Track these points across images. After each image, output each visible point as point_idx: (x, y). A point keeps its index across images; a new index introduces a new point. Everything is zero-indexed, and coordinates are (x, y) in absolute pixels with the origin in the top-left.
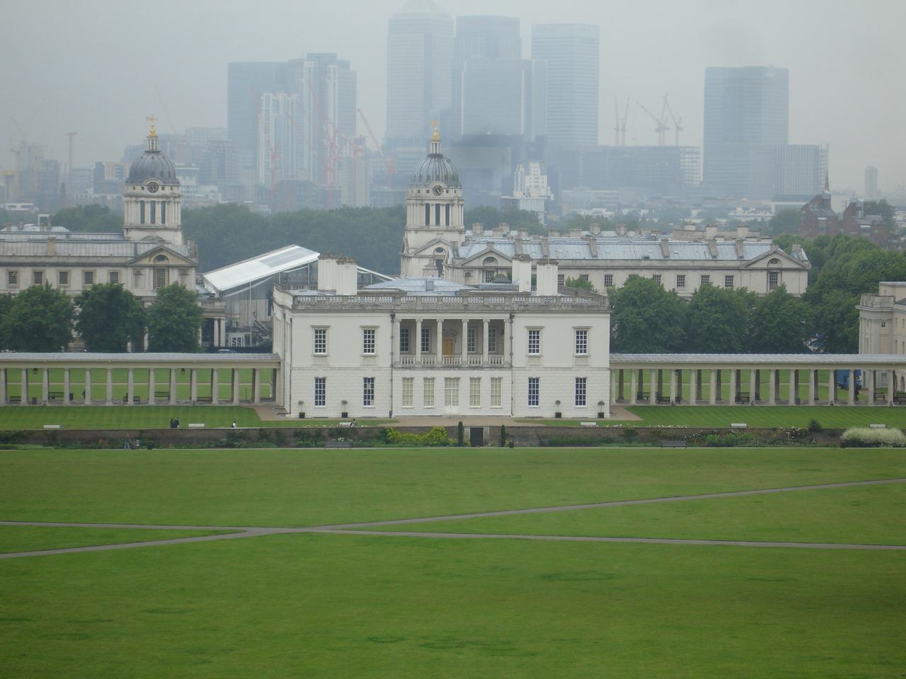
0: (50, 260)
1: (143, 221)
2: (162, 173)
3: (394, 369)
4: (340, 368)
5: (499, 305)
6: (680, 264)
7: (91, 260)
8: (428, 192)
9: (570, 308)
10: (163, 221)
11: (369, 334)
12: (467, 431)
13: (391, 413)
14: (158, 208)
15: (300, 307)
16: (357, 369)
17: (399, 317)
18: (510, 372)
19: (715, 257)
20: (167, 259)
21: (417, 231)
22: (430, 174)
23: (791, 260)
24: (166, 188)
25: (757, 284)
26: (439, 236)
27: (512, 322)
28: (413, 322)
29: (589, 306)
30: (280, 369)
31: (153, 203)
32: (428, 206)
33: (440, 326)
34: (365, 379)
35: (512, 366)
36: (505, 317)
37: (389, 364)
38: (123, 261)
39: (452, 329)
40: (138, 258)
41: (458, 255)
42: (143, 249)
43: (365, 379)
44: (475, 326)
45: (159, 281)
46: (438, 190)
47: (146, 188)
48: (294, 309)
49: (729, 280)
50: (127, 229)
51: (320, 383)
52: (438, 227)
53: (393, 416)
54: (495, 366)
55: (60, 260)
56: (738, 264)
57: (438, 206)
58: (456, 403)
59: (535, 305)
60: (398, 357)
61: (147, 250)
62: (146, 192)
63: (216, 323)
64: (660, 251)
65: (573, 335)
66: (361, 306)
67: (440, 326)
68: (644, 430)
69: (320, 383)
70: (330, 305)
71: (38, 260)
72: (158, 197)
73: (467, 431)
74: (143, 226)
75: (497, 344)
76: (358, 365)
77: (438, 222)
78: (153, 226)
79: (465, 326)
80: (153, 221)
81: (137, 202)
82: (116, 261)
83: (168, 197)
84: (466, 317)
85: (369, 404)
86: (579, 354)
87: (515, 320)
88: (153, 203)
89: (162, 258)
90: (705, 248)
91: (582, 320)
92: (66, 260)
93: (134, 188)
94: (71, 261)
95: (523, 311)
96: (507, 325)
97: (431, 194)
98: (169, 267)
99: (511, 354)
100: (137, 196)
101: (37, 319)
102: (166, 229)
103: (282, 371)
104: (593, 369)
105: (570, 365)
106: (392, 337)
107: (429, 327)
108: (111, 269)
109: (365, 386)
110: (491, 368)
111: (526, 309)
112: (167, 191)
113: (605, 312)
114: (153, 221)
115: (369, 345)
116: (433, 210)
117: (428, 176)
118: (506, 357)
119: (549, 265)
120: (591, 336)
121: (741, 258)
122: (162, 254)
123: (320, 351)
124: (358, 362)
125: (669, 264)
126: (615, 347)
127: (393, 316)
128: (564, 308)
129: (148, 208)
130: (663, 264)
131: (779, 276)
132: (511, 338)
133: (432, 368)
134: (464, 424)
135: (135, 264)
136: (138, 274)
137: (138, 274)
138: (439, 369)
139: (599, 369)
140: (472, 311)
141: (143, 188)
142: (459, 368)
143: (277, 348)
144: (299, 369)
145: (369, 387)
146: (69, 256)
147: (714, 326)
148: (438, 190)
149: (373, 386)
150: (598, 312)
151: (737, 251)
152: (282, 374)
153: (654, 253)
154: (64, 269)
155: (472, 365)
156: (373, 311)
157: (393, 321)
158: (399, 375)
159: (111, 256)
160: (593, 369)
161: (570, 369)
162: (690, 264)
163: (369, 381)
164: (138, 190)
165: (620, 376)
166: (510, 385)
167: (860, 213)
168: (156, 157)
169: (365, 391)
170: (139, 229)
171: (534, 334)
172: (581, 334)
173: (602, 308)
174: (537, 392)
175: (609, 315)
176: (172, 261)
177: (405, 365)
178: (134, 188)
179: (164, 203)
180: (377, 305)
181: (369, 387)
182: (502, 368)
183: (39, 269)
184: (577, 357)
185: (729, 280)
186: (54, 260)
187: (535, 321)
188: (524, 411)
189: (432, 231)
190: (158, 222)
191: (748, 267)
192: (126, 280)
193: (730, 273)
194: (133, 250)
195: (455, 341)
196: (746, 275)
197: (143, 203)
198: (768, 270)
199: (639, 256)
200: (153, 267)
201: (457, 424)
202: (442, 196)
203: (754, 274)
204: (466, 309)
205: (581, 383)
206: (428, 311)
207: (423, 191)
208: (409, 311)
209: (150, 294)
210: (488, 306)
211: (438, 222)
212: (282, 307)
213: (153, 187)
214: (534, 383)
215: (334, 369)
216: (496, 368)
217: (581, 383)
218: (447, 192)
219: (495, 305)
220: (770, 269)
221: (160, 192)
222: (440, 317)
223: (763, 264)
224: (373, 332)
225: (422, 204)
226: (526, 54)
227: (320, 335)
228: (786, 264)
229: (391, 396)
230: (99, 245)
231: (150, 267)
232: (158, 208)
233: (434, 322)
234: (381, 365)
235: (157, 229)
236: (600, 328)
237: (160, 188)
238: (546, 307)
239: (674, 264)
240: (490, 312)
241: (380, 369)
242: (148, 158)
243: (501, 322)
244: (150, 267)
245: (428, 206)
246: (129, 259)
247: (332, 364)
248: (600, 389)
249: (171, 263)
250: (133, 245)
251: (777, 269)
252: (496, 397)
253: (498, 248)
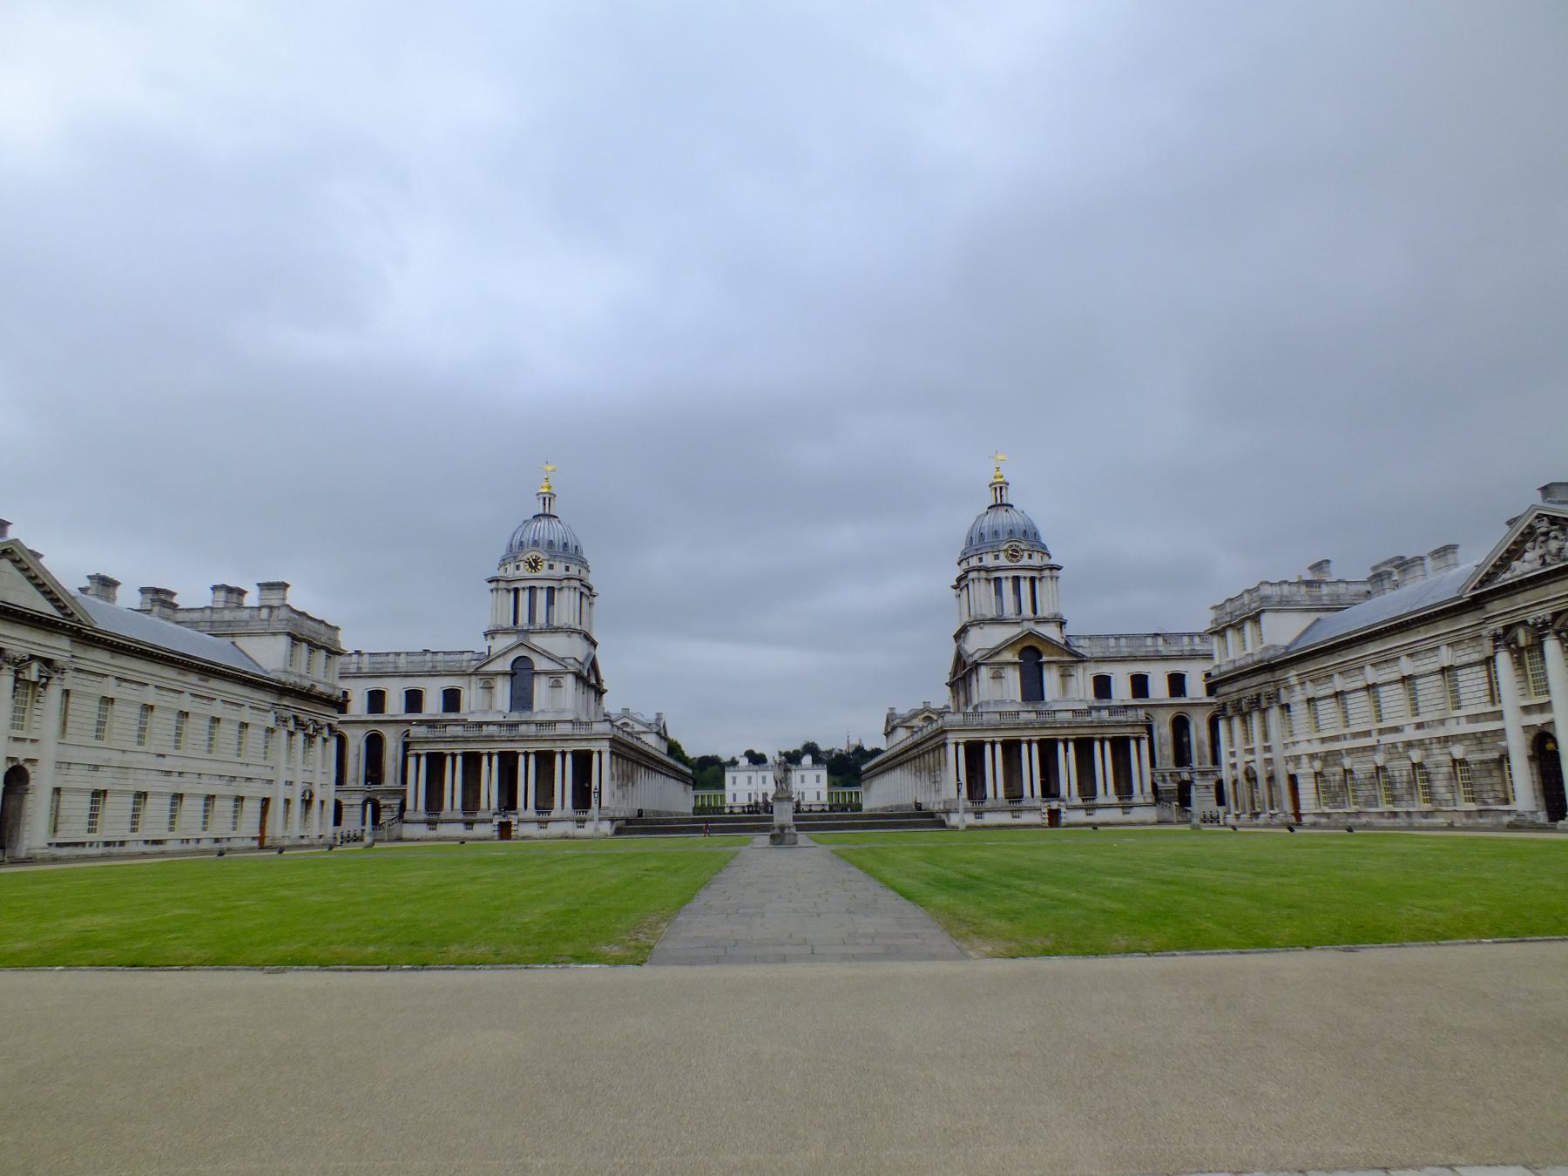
10: (1035, 611)
14: (1025, 586)
24: (1035, 555)
31: (1016, 579)
47: (1002, 555)
62: (1003, 561)
81: (988, 580)
83: (1041, 569)
88: (1016, 579)
100: (987, 570)
112: (1037, 560)
141: (997, 557)
164: (989, 561)
178: (981, 560)
179: (1033, 580)
197: (998, 580)
232: (1025, 586)
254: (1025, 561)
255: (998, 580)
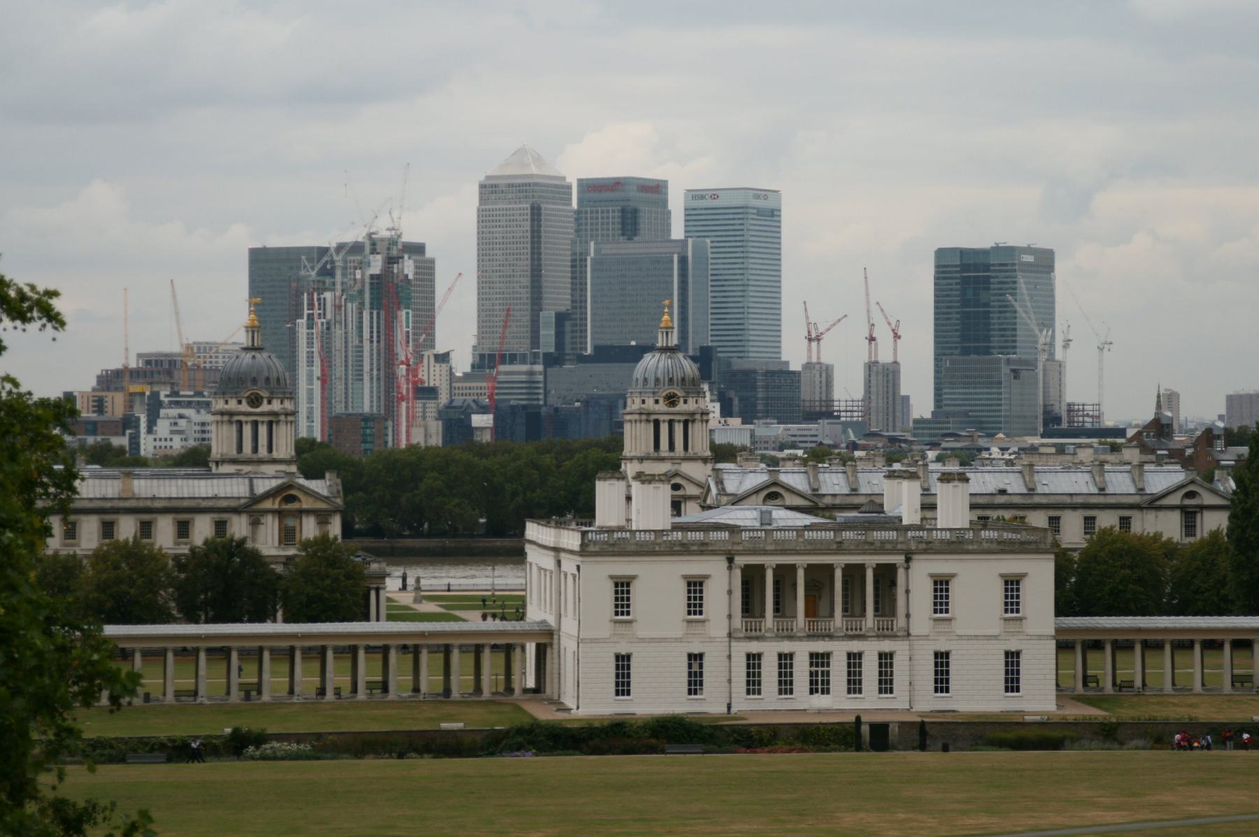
0: (127, 504)
1: (240, 448)
2: (267, 379)
3: (733, 644)
4: (652, 640)
5: (888, 541)
6: (1052, 500)
7: (186, 504)
8: (657, 402)
9: (994, 546)
10: (270, 449)
11: (695, 586)
12: (865, 729)
13: (729, 707)
14: (263, 430)
15: (592, 548)
16: (677, 640)
17: (741, 560)
18: (907, 643)
19: (1102, 489)
20: (300, 501)
21: (641, 460)
22: (660, 375)
23: (1215, 492)
25: (1169, 526)
26: (676, 467)
27: (907, 568)
28: (761, 569)
29: (1022, 543)
30: (551, 644)
31: (255, 425)
32: (657, 424)
33: (801, 574)
34: (690, 656)
35: (909, 635)
36: (898, 559)
37: (725, 632)
38: (233, 504)
39: (819, 578)
40: (256, 499)
41: (724, 489)
42: (262, 487)
43: (690, 656)
44: (854, 574)
45: (287, 536)
46: (671, 400)
47: (244, 401)
48: (584, 550)
49: (1125, 522)
50: (217, 463)
51: (623, 662)
52: (672, 454)
53: (734, 710)
54: (885, 633)
55: (141, 504)
56: (1137, 499)
57: (671, 423)
58: (826, 691)
59: (942, 541)
60: (738, 621)
61: (267, 488)
62: (244, 407)
63: (373, 594)
64: (1021, 483)
65: (999, 587)
66: (683, 545)
67: (801, 574)
68: (1097, 730)
69: (623, 662)
70: (637, 544)
71: (108, 505)
72: (262, 414)
73: (865, 729)
74: (240, 457)
75: (886, 605)
76: (679, 633)
77: (672, 447)
78: (255, 457)
79: (838, 574)
80: (255, 449)
81: (230, 422)
82: (224, 504)
83: (276, 414)
84: (839, 561)
85: (696, 693)
86: (1009, 615)
87: (913, 565)
88: (255, 425)
89: (292, 499)
90: (1087, 477)
91: (1013, 565)
92: (149, 504)
93: (227, 402)
94: (157, 504)
95: (925, 552)
96: (901, 573)
97: (662, 407)
98: (301, 513)
99: (908, 616)
100: (231, 414)
101: (124, 587)
102: (275, 461)
103: (555, 646)
104: (1032, 637)
105: (995, 631)
106: (730, 592)
107: (784, 575)
108: (216, 516)
109: (690, 666)
110: (878, 636)
111: (930, 548)
112: (276, 406)
113: (1046, 552)
114: (255, 449)
115: (695, 604)
116: (664, 429)
117: (657, 380)
118: (900, 621)
119: (956, 483)
120: (1026, 588)
121: (1141, 491)
122: (293, 492)
123: (622, 614)
124: (679, 630)
125: (1037, 500)
126: (1063, 607)
127: (730, 561)
128: (985, 545)
129: (247, 431)
130: (1028, 501)
131: (1199, 516)
132: (907, 592)
133: (791, 638)
134: (864, 719)
135: (251, 508)
136: (255, 523)
137: (255, 523)
138: (800, 639)
139: (1040, 637)
140: (850, 553)
141: (240, 402)
142: (831, 637)
143: (536, 613)
144: (593, 641)
145: (695, 668)
146: (154, 498)
147: (1121, 587)
148: (671, 400)
149: (701, 666)
150: (1037, 551)
151: (1134, 481)
152: (556, 651)
153: (1015, 485)
154: (146, 517)
155: (850, 632)
156: (701, 553)
157: (730, 568)
158: (742, 649)
159: (216, 498)
160: (1032, 637)
161: (996, 637)
162: (1068, 500)
163: (695, 659)
164: (233, 405)
165: (1064, 646)
166: (907, 663)
167: (1219, 445)
168: (258, 355)
169: (690, 674)
170: (234, 461)
171: (941, 586)
172: (1012, 585)
173: (1042, 546)
174: (948, 672)
175: (1053, 556)
176: (306, 503)
177: (749, 633)
178: (227, 402)
179: (270, 424)
180: (707, 544)
181: (695, 668)
182: (894, 637)
183: (108, 517)
184: (1006, 619)
185: (1125, 522)
186: (133, 504)
187: (942, 565)
188: (927, 702)
189: (663, 459)
190: (262, 451)
191: (1154, 504)
192: (239, 527)
193: (1126, 513)
194: (247, 488)
195: (820, 598)
196: (1150, 516)
197: (240, 423)
198: (1182, 508)
199: (991, 489)
200: (280, 513)
201: (853, 719)
202: (677, 409)
203: (1161, 514)
204: (840, 548)
205: (1012, 659)
206: (783, 552)
207: (650, 403)
208: (754, 552)
209: (274, 552)
210: (872, 544)
211: (672, 447)
212: (557, 550)
213: (255, 401)
214: (942, 659)
215: (643, 640)
216: (885, 637)
217: (1012, 659)
218: (685, 402)
219: (883, 542)
220: (1186, 506)
221: (265, 407)
222: (801, 561)
223: (1175, 500)
224: (701, 584)
225: (648, 421)
226: (677, 231)
227: (622, 587)
228: (1208, 499)
229: (730, 681)
230: (196, 482)
231: (273, 512)
232: (263, 430)
233: (792, 568)
234: (713, 633)
235: (261, 462)
236: (1040, 578)
237: (265, 401)
238: (956, 545)
239: (1044, 500)
240: (876, 552)
241: (712, 640)
242: (247, 358)
243: (892, 568)
244: (273, 512)
245: (657, 424)
246: (243, 501)
247: (641, 634)
248: (1040, 667)
249: (305, 506)
250: (247, 481)
251: (1196, 506)
252: (886, 685)
253: (783, 478)
254: (265, 407)
255: (240, 423)
